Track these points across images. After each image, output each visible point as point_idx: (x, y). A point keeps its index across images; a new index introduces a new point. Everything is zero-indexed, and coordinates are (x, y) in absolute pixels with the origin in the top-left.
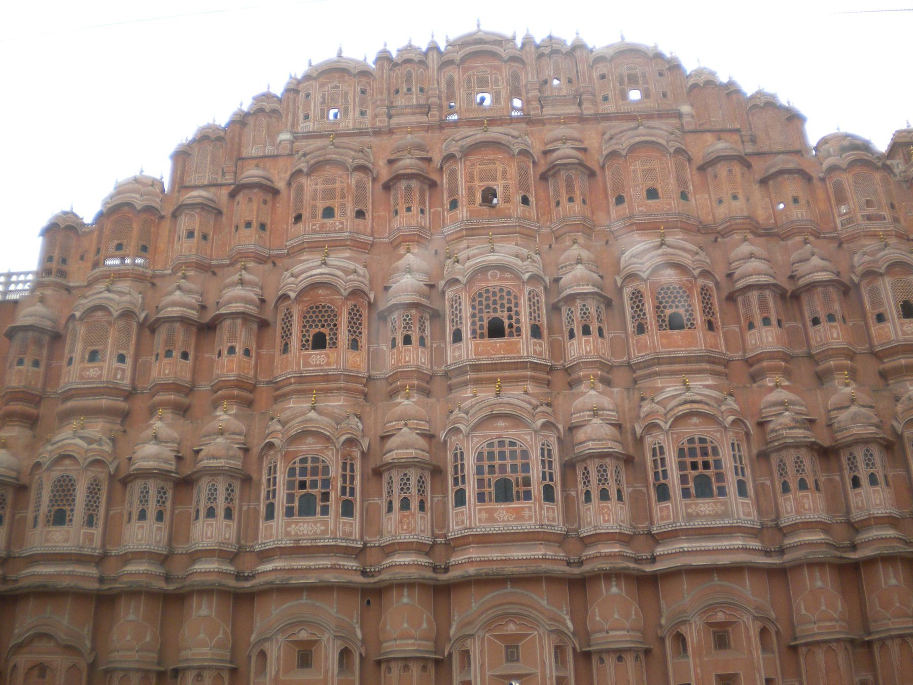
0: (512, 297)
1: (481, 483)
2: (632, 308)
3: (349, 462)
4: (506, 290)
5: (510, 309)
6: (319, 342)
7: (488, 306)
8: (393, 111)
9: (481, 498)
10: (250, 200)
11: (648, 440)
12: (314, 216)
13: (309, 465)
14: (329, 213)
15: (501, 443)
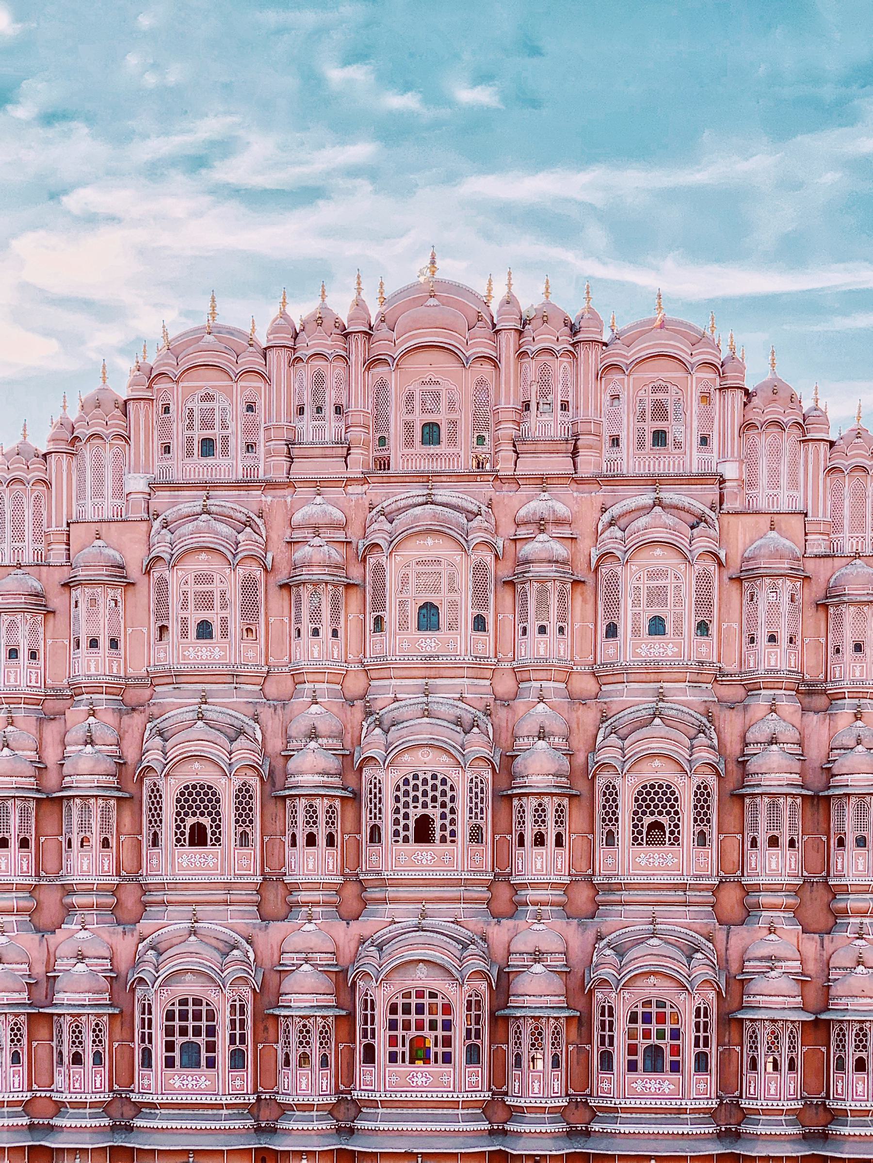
0: (447, 788)
1: (393, 1041)
2: (604, 807)
3: (238, 1003)
4: (440, 777)
5: (443, 805)
6: (198, 837)
7: (416, 799)
8: (295, 452)
9: (393, 1057)
10: (93, 601)
11: (598, 995)
12: (184, 634)
13: (190, 1008)
14: (204, 630)
15: (420, 994)
